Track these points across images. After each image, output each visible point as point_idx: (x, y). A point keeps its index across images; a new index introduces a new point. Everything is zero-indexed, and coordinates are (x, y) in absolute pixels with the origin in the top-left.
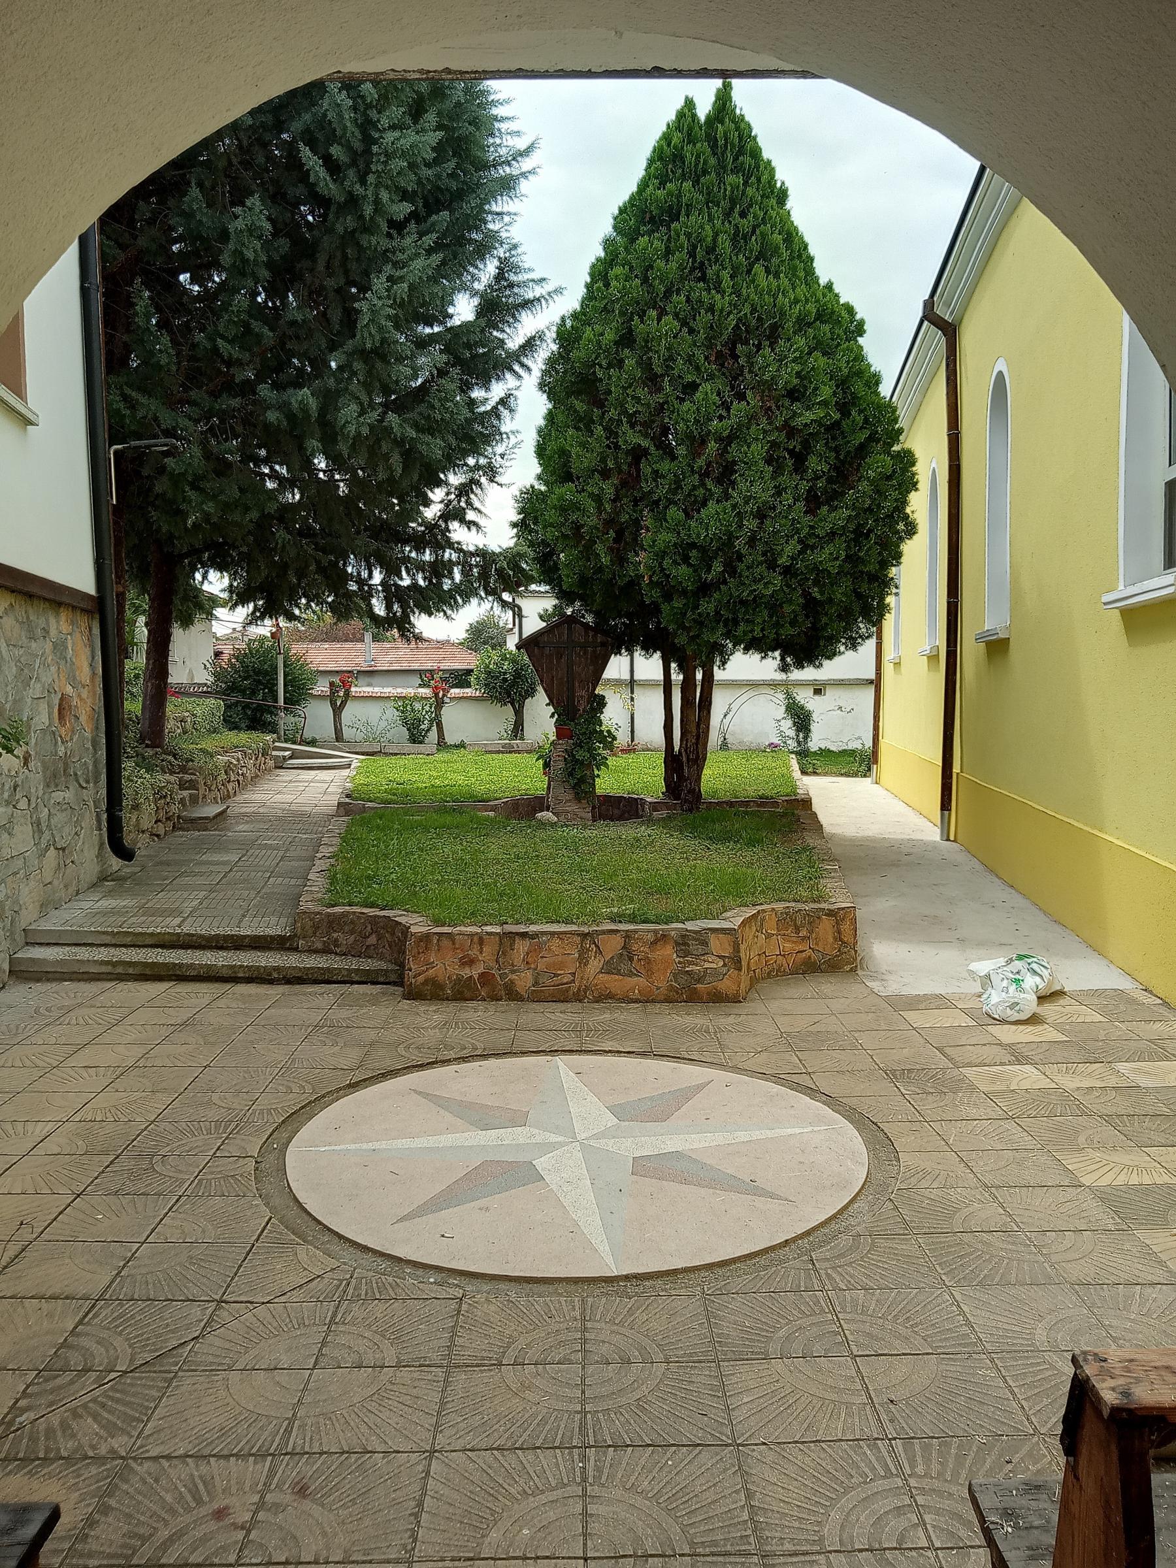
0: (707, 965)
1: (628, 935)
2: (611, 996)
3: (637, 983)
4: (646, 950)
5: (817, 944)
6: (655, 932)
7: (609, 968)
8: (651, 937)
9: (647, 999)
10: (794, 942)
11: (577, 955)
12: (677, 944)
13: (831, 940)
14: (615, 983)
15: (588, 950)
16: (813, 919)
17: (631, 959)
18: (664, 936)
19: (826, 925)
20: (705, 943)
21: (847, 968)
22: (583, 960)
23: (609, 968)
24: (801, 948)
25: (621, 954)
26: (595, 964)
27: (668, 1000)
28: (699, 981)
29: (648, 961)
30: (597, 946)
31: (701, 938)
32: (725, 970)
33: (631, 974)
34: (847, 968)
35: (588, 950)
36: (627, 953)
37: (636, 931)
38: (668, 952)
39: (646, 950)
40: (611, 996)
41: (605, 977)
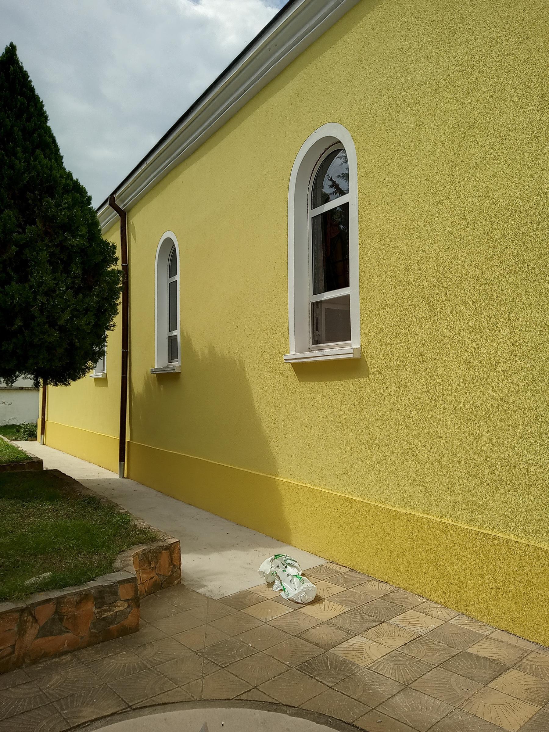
0: (117, 609)
1: (59, 601)
2: (46, 655)
3: (65, 639)
4: (73, 609)
5: (160, 571)
6: (79, 593)
7: (44, 632)
8: (76, 598)
9: (74, 649)
10: (148, 573)
11: (16, 629)
12: (96, 599)
13: (167, 566)
14: (47, 643)
15: (26, 622)
16: (157, 553)
17: (61, 620)
18: (86, 595)
19: (165, 555)
20: (115, 593)
21: (176, 582)
22: (21, 632)
23: (44, 632)
24: (151, 575)
25: (53, 619)
26: (32, 631)
27: (90, 644)
28: (111, 624)
29: (74, 617)
30: (34, 617)
31: (112, 590)
32: (129, 609)
33: (61, 632)
34: (176, 582)
35: (26, 622)
36: (58, 616)
37: (64, 597)
38: (90, 607)
39: (73, 609)
40: (46, 655)
41: (40, 641)
